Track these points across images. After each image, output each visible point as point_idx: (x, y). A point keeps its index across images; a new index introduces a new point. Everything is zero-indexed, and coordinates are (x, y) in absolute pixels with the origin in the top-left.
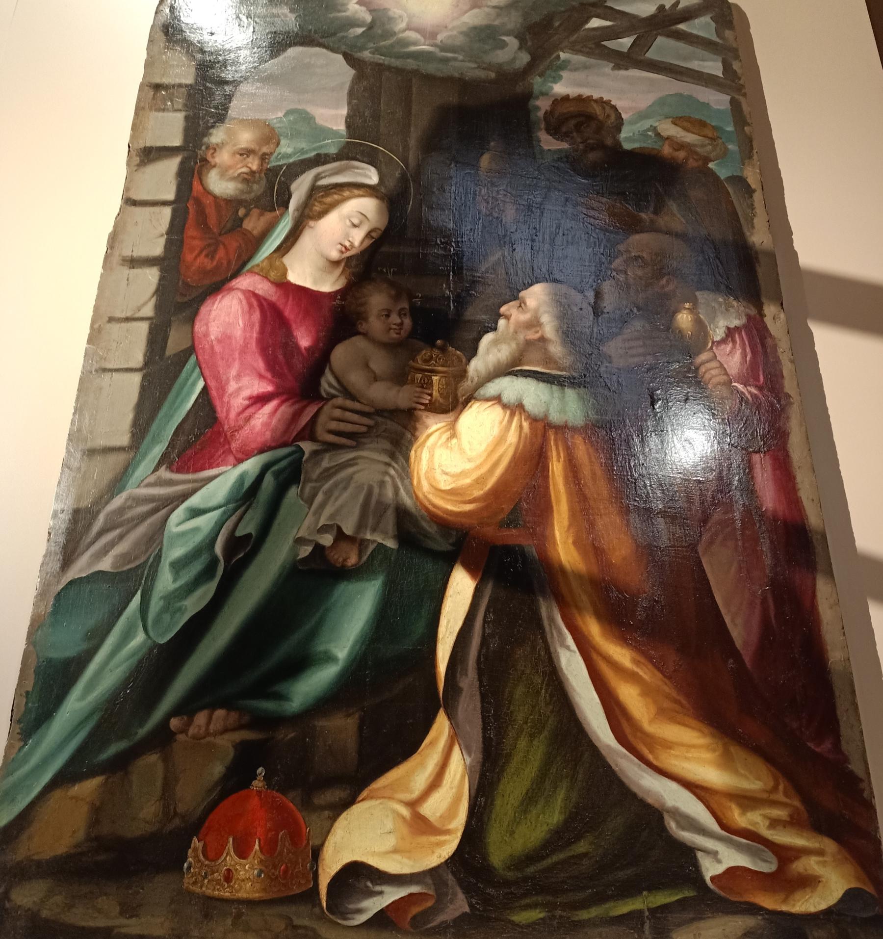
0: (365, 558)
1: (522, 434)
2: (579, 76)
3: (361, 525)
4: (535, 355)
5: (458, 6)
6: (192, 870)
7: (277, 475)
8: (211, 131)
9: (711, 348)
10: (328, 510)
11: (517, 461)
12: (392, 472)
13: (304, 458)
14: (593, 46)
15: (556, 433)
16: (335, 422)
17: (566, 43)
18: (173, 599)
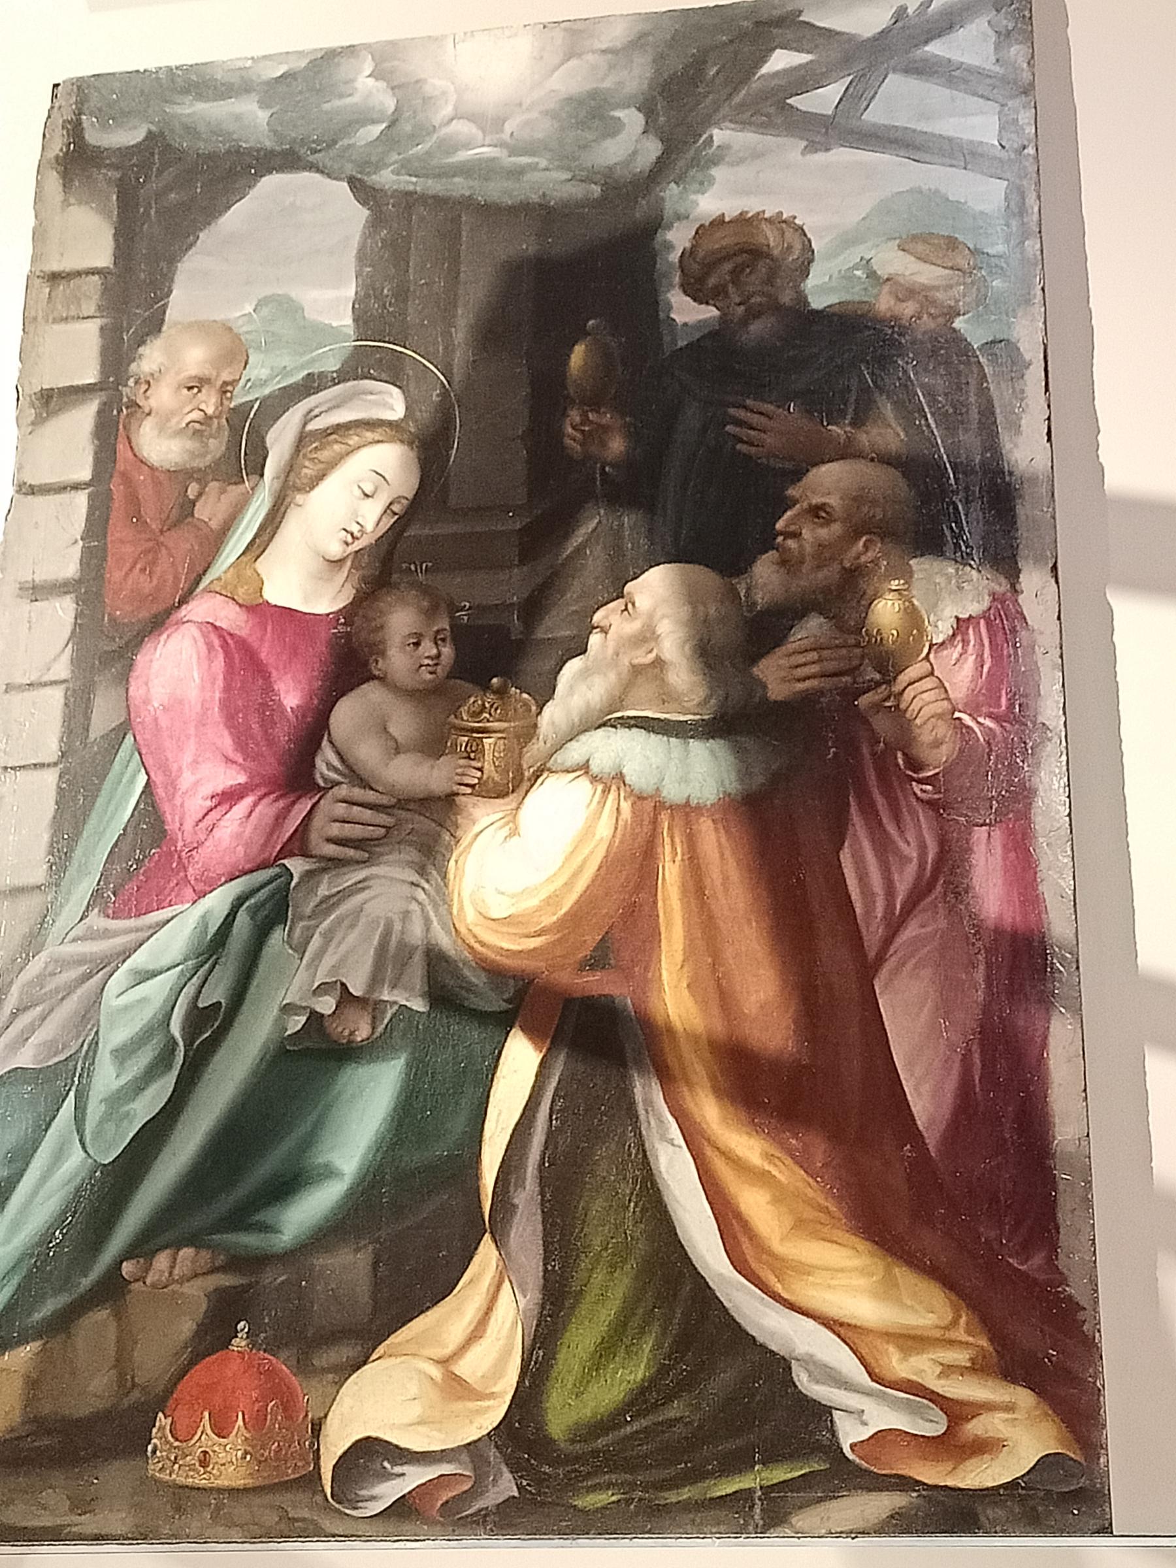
0: (380, 1029)
1: (620, 822)
2: (745, 172)
3: (375, 980)
4: (645, 688)
5: (542, 57)
6: (158, 1453)
7: (254, 912)
8: (141, 350)
9: (927, 657)
10: (328, 961)
11: (609, 865)
12: (421, 896)
13: (293, 884)
14: (772, 110)
15: (672, 817)
16: (338, 824)
17: (725, 110)
18: (118, 1100)
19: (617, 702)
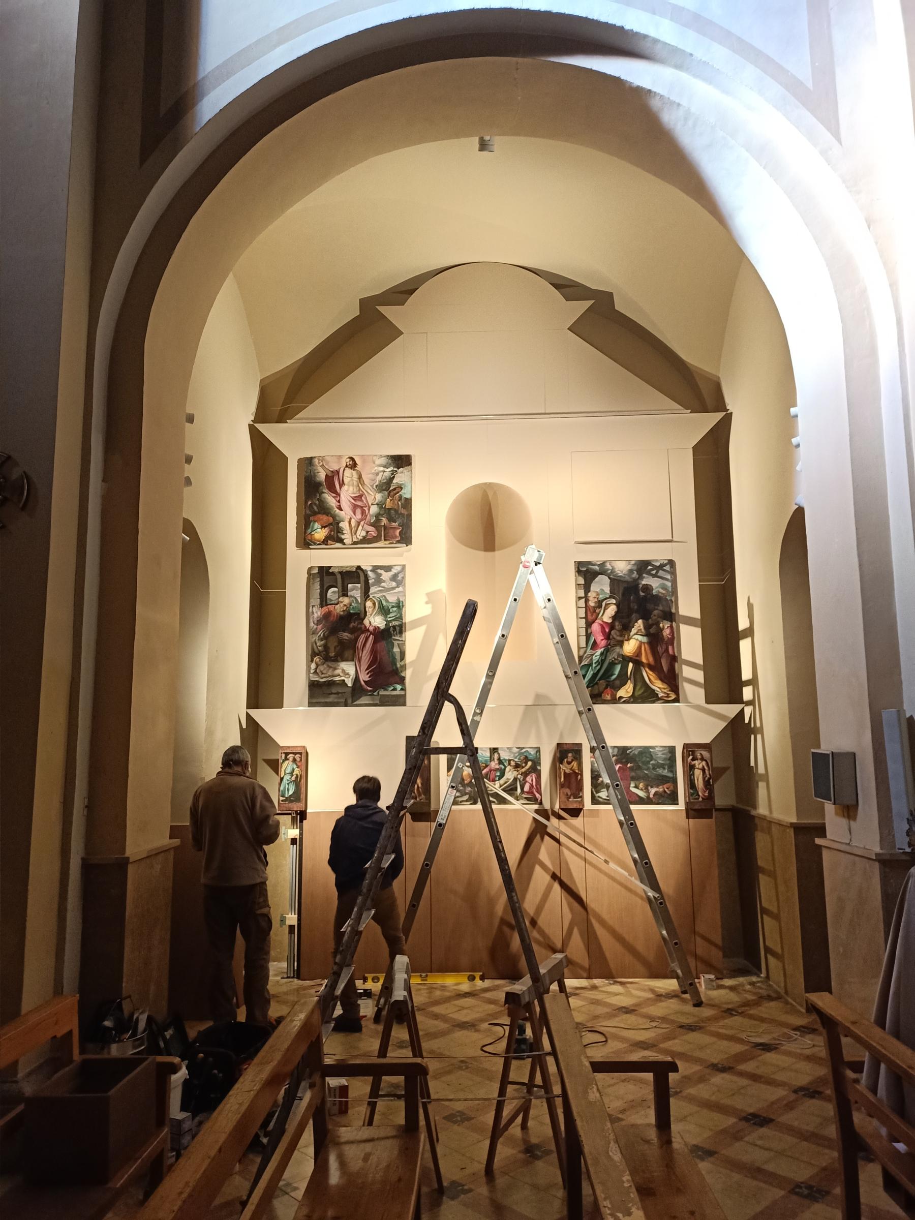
19: (637, 632)
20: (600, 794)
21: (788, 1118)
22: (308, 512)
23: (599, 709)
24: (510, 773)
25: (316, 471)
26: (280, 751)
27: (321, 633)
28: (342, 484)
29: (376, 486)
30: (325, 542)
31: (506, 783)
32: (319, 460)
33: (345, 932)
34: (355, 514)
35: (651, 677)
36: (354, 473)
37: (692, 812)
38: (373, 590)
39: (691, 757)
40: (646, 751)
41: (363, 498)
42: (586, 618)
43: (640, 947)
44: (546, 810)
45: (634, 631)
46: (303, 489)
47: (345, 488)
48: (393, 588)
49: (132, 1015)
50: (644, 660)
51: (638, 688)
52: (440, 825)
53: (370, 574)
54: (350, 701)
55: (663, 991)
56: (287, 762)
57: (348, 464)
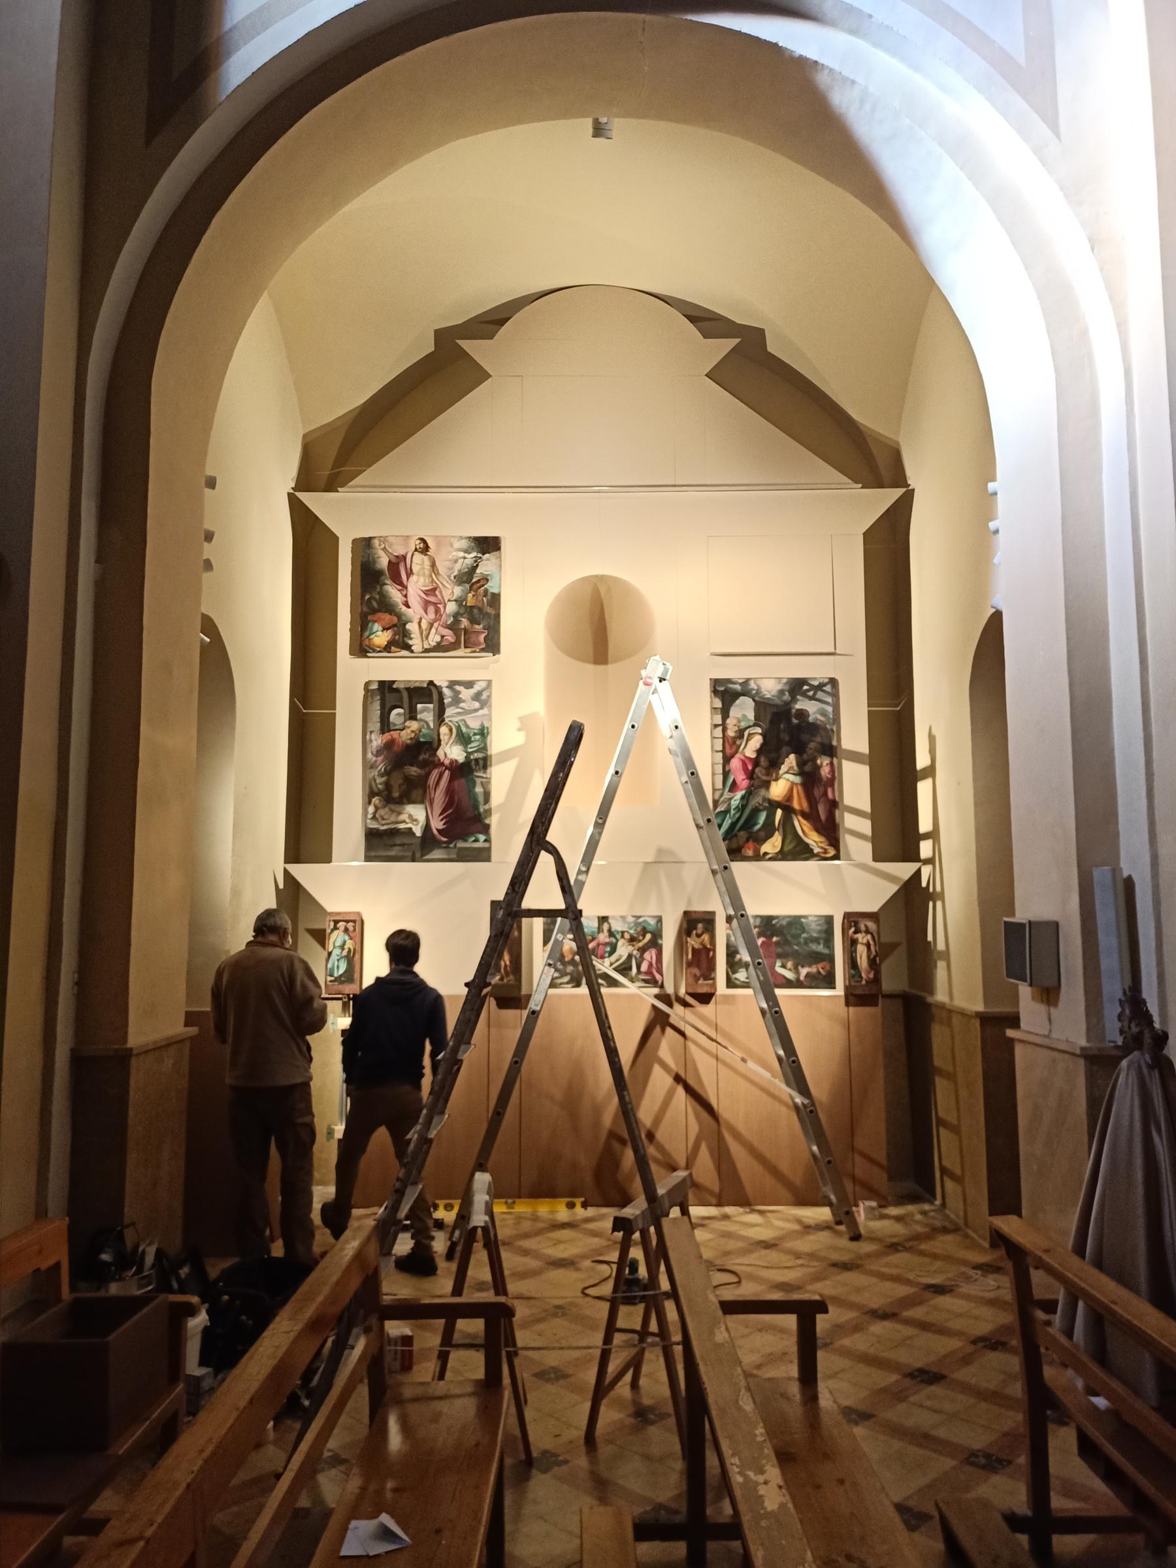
19: (789, 770)
20: (737, 976)
21: (965, 1374)
22: (365, 609)
23: (737, 867)
24: (624, 947)
25: (376, 556)
26: (328, 918)
27: (382, 767)
28: (410, 573)
29: (455, 577)
30: (387, 648)
31: (617, 960)
32: (380, 541)
33: (410, 1140)
34: (426, 613)
35: (805, 829)
36: (426, 558)
37: (853, 998)
38: (449, 712)
39: (853, 929)
40: (796, 922)
41: (437, 592)
42: (723, 751)
43: (785, 1167)
44: (668, 996)
45: (784, 768)
46: (359, 578)
47: (413, 578)
48: (476, 710)
49: (137, 1247)
50: (796, 805)
51: (788, 841)
52: (533, 1012)
53: (446, 691)
54: (418, 855)
55: (811, 1222)
56: (336, 932)
57: (418, 547)
